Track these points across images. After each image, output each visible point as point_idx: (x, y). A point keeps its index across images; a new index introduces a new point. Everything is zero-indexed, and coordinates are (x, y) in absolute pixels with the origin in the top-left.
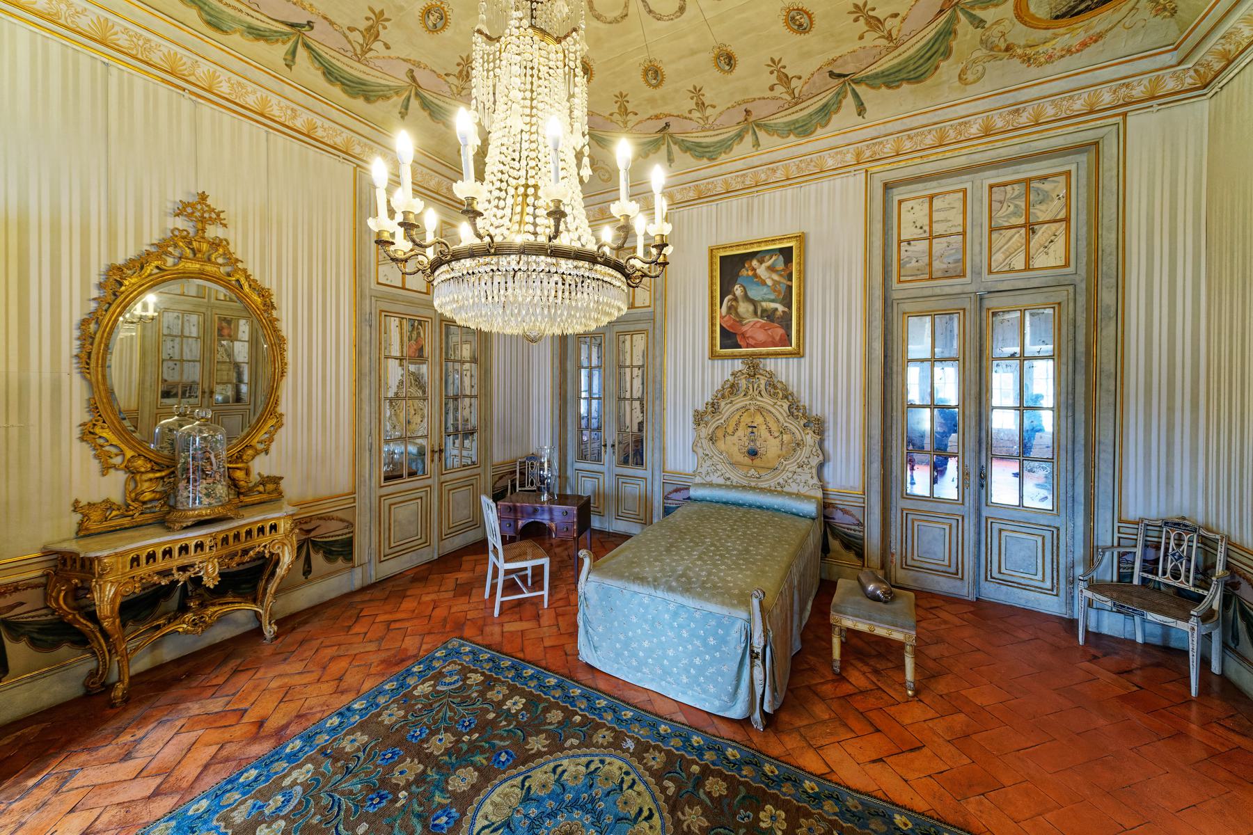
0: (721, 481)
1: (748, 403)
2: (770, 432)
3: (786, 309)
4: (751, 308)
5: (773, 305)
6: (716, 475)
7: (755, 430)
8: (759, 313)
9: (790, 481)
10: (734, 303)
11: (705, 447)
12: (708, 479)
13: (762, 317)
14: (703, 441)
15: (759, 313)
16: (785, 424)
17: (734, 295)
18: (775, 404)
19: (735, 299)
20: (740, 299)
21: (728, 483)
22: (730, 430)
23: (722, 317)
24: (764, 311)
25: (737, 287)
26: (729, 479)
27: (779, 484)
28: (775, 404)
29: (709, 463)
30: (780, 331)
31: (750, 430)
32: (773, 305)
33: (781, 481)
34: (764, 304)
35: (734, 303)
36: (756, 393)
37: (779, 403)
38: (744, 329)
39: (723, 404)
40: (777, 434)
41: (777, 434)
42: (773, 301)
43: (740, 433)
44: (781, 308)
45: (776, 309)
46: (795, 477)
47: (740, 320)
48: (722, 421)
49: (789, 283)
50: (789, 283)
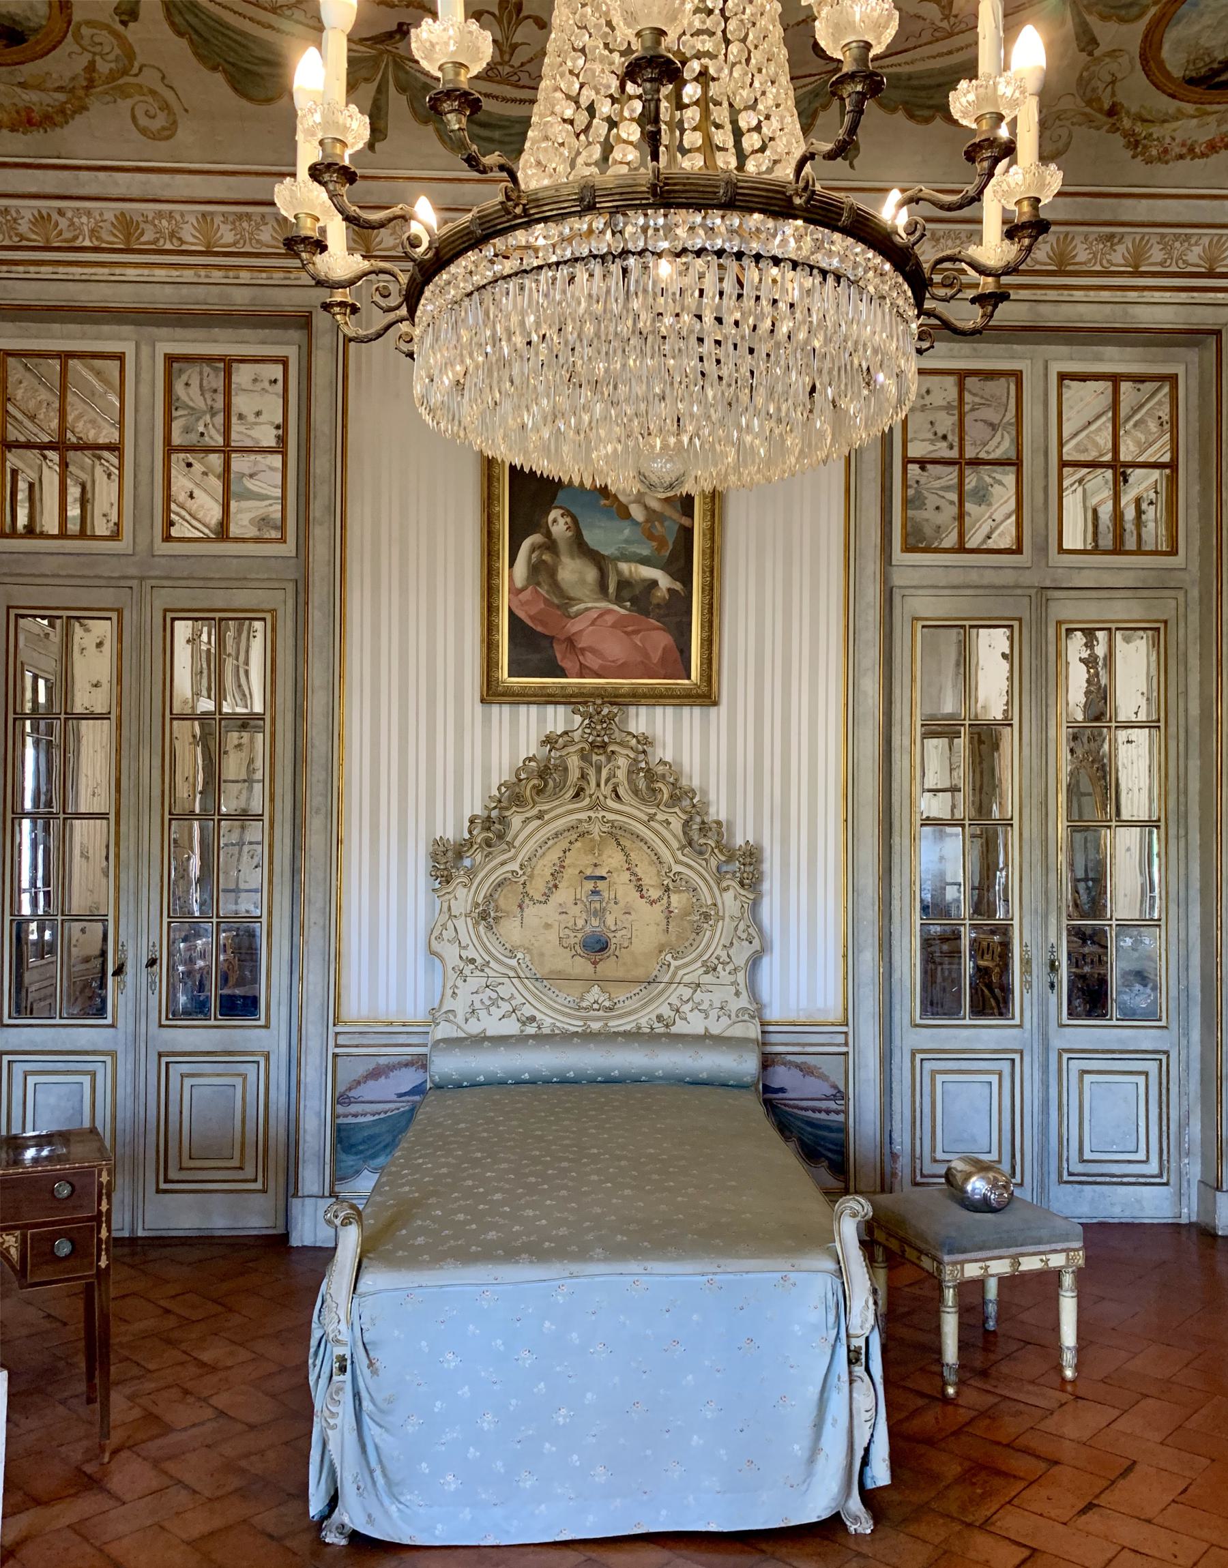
0: (511, 1027)
1: (583, 816)
2: (640, 888)
3: (678, 586)
4: (591, 574)
5: (648, 572)
6: (497, 1013)
7: (601, 885)
8: (612, 589)
9: (686, 1008)
10: (546, 557)
11: (465, 940)
12: (474, 1028)
13: (619, 600)
14: (460, 923)
15: (612, 589)
16: (677, 868)
17: (548, 534)
18: (652, 817)
19: (550, 545)
20: (562, 546)
21: (530, 1030)
22: (537, 887)
23: (514, 592)
24: (623, 584)
25: (554, 514)
26: (532, 1019)
27: (660, 1018)
28: (652, 817)
29: (476, 982)
30: (661, 640)
31: (589, 885)
32: (648, 572)
33: (666, 1011)
34: (624, 567)
35: (546, 557)
36: (606, 790)
37: (660, 817)
38: (574, 627)
39: (516, 821)
40: (654, 894)
41: (654, 894)
42: (645, 561)
43: (563, 895)
44: (664, 581)
45: (654, 583)
46: (698, 996)
47: (564, 601)
48: (515, 866)
49: (685, 521)
50: (685, 521)
